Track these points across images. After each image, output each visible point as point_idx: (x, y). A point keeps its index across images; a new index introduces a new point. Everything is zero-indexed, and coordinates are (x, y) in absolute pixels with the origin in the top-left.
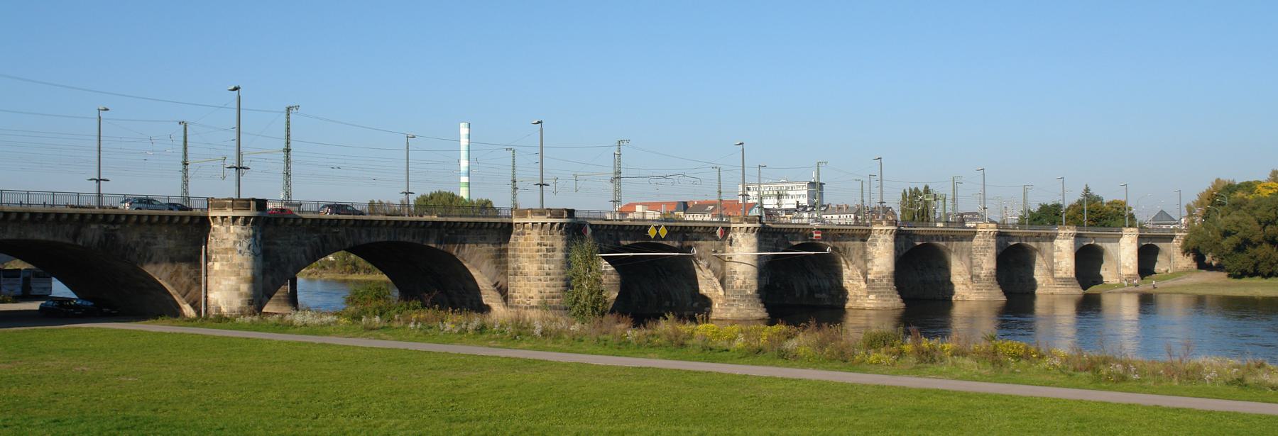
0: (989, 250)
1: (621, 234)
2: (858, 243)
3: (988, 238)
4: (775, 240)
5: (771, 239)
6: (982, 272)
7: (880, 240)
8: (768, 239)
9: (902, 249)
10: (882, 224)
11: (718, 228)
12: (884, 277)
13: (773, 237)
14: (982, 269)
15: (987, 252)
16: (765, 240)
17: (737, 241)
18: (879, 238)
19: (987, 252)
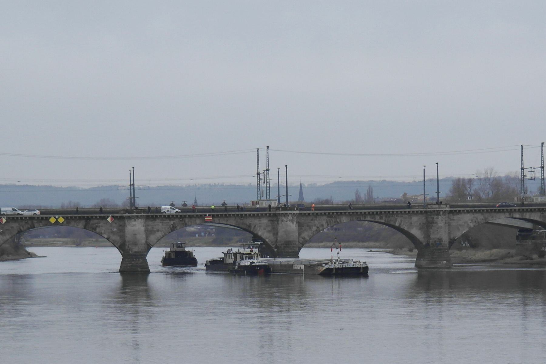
0: (434, 225)
1: (35, 221)
2: (265, 221)
3: (433, 216)
4: (172, 222)
5: (168, 222)
6: (430, 241)
7: (280, 220)
8: (166, 222)
9: (323, 225)
10: (279, 209)
11: (109, 216)
12: (282, 245)
13: (170, 220)
14: (430, 238)
15: (432, 226)
16: (162, 223)
17: (126, 224)
18: (279, 219)
19: (432, 226)
